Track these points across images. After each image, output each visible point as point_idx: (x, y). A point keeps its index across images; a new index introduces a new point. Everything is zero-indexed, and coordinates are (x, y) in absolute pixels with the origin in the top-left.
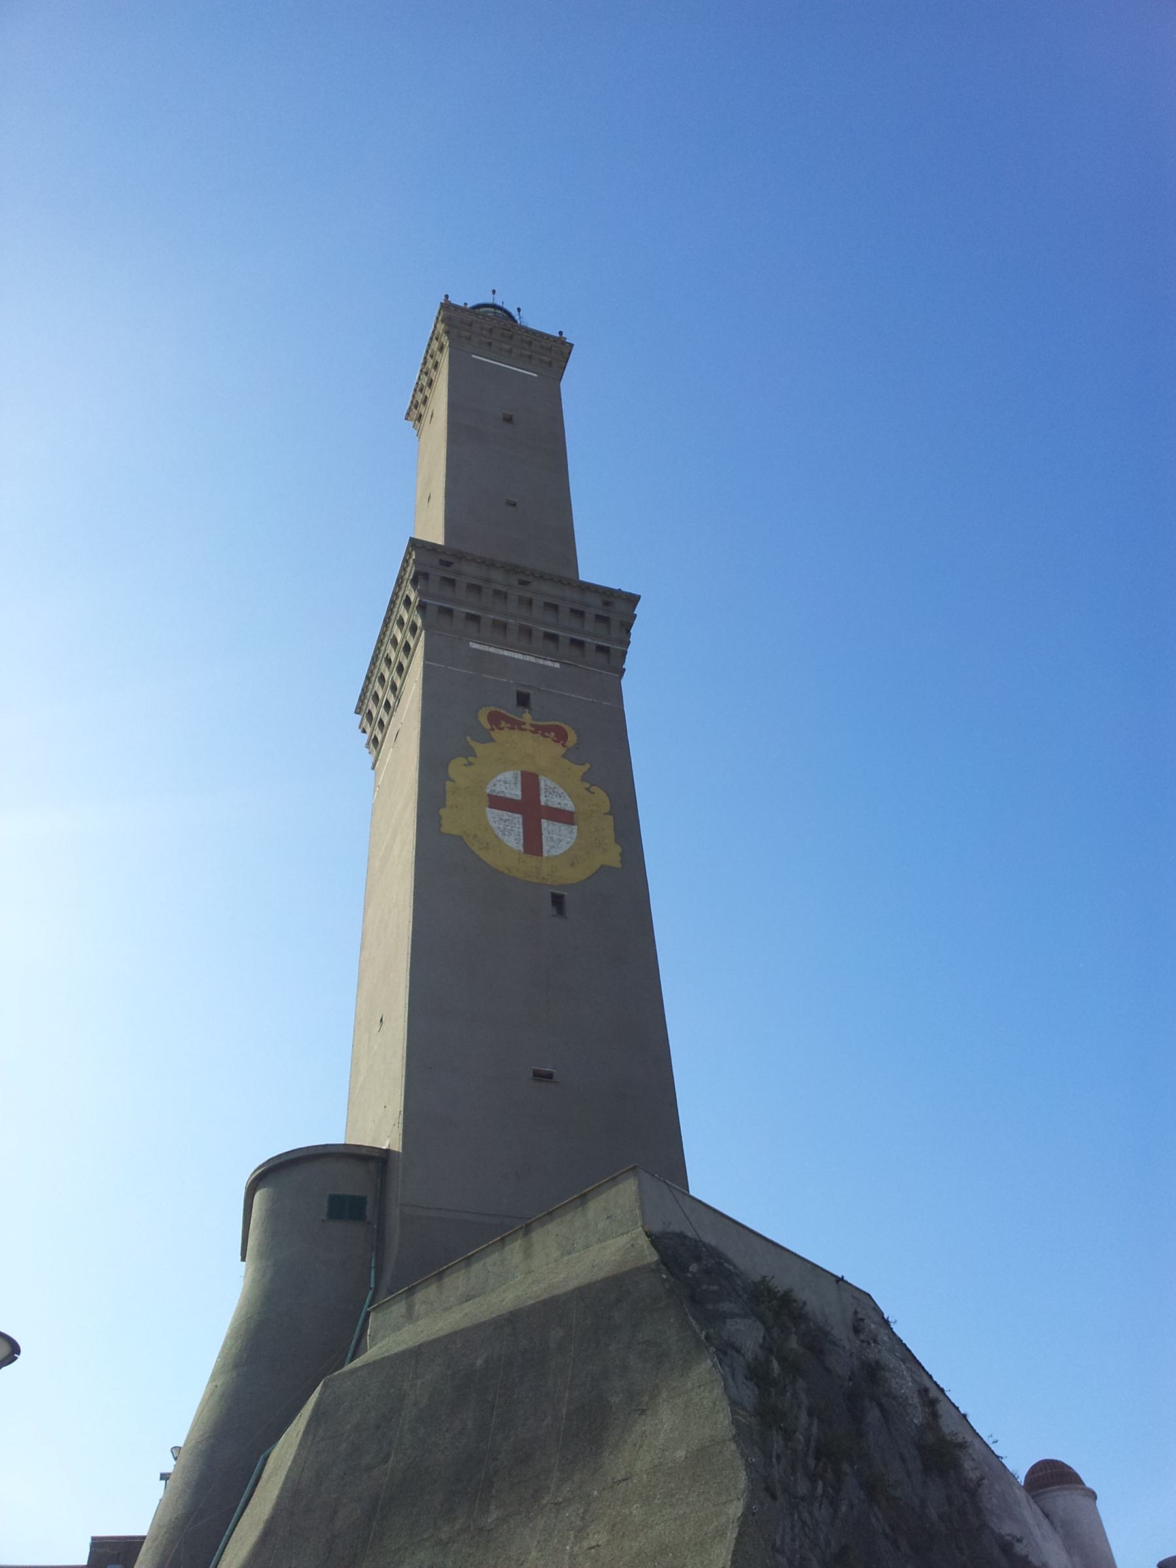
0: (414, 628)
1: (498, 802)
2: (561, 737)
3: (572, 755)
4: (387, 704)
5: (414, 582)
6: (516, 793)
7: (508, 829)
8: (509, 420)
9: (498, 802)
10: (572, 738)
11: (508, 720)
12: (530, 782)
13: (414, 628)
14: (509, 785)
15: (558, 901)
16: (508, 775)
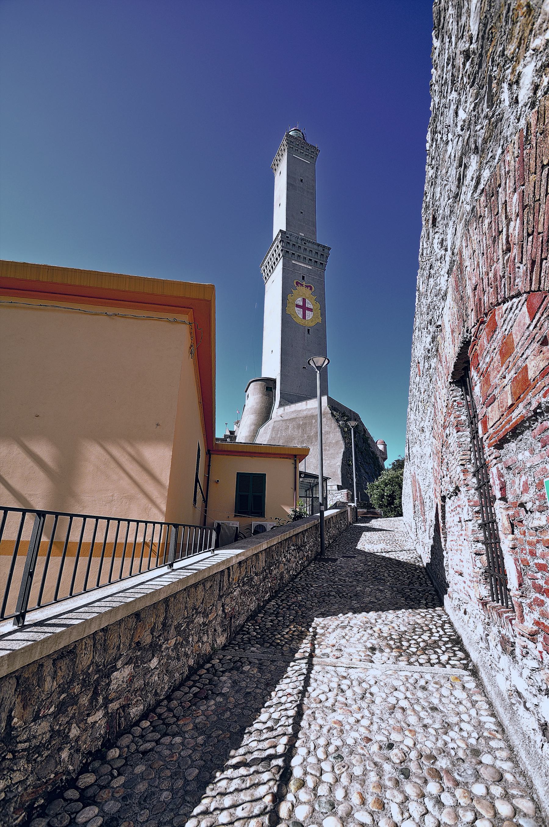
0: (279, 255)
1: (297, 306)
2: (311, 289)
3: (313, 294)
4: (270, 271)
5: (280, 242)
6: (301, 304)
7: (299, 312)
8: (302, 181)
9: (297, 306)
10: (313, 288)
11: (300, 284)
12: (304, 300)
13: (279, 255)
14: (300, 302)
15: (308, 330)
16: (300, 299)
